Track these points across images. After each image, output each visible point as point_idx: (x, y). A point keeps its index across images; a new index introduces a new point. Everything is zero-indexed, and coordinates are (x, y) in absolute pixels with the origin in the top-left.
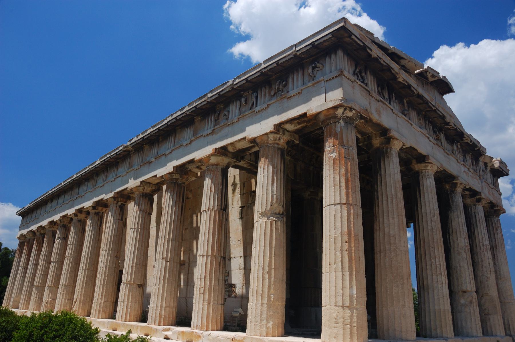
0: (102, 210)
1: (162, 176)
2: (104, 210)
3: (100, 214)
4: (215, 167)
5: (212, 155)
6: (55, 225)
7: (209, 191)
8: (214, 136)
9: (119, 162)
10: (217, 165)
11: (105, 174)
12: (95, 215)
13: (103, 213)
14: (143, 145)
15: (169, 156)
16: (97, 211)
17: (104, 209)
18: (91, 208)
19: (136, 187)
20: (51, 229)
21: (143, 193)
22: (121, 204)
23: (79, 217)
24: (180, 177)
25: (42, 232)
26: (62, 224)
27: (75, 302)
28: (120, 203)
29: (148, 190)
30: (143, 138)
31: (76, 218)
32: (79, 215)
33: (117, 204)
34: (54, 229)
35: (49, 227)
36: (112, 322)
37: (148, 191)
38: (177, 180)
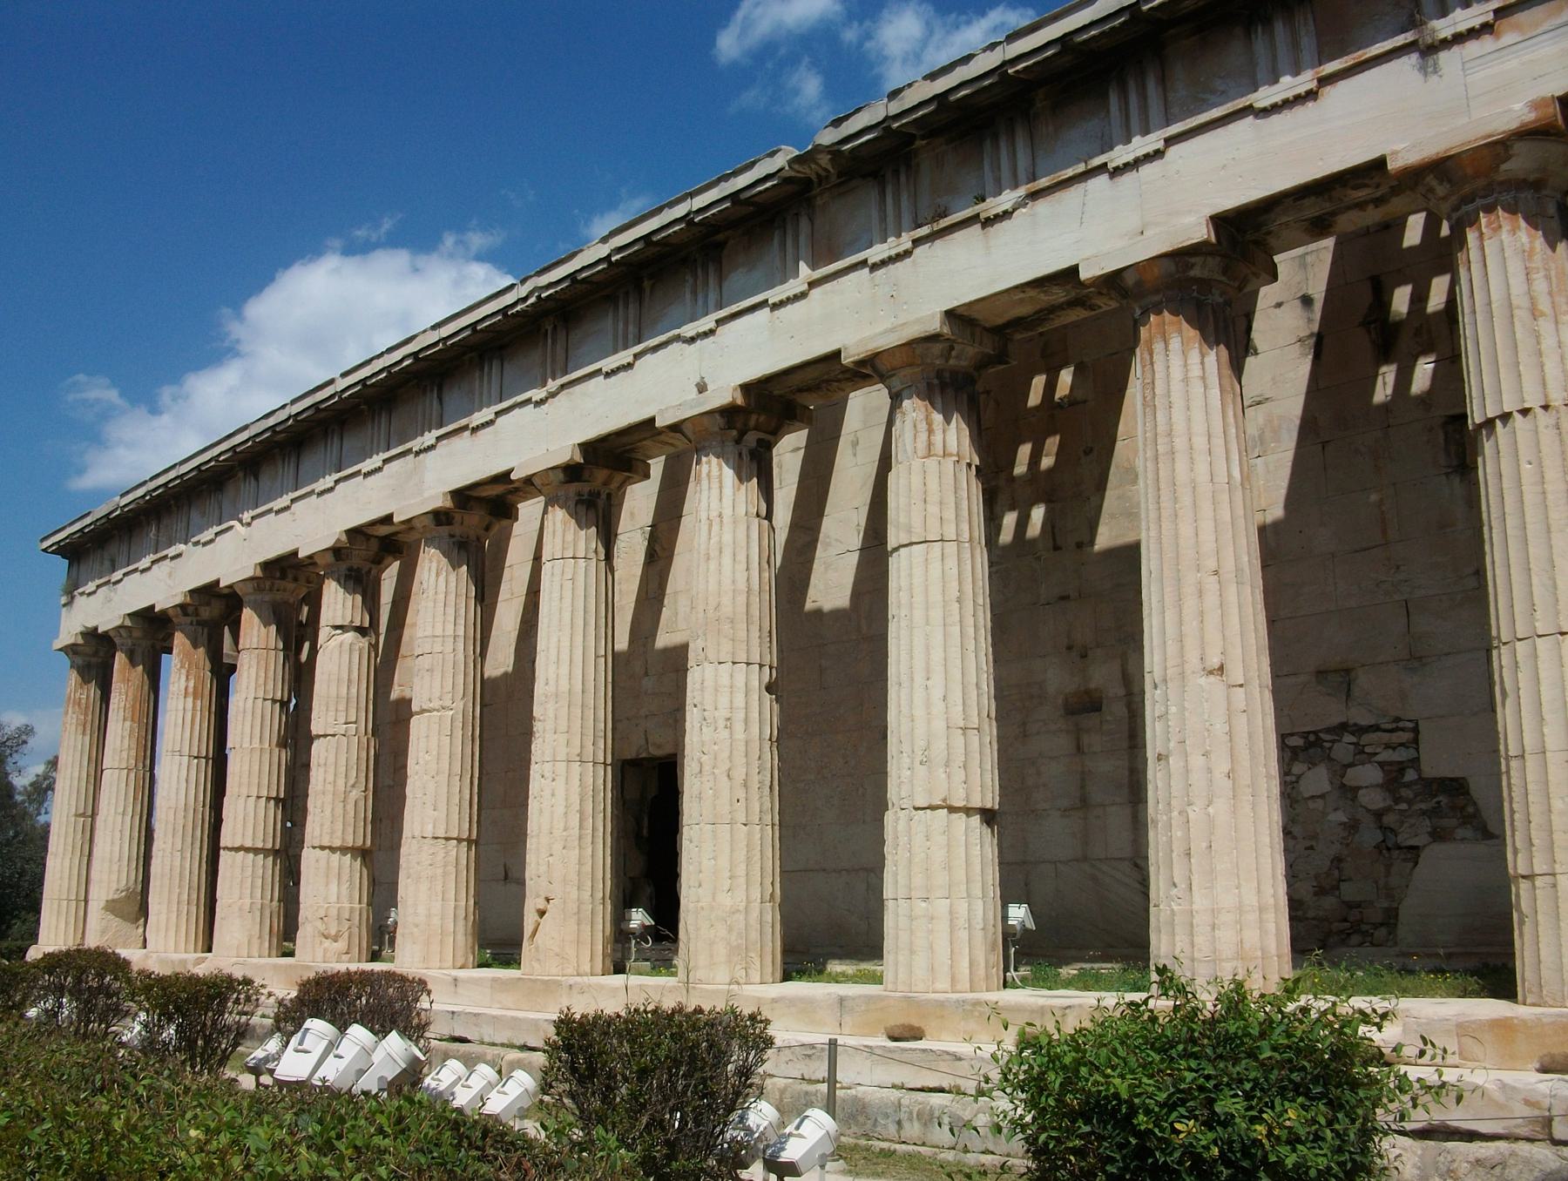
0: (605, 484)
1: (1119, 273)
2: (614, 485)
3: (601, 503)
4: (1527, 195)
5: (1527, 134)
6: (283, 577)
7: (1521, 315)
8: (1508, 38)
9: (721, 246)
10: (1537, 185)
11: (632, 310)
12: (582, 509)
13: (609, 496)
14: (911, 138)
15: (1147, 170)
16: (585, 488)
17: (619, 477)
18: (561, 476)
19: (910, 344)
20: (267, 598)
21: (939, 374)
22: (759, 441)
23: (457, 529)
24: (1225, 272)
25: (206, 613)
26: (343, 566)
27: (542, 913)
28: (751, 438)
29: (967, 353)
30: (941, 98)
31: (445, 530)
32: (458, 517)
33: (738, 442)
34: (278, 596)
35: (259, 589)
36: (869, 999)
37: (964, 363)
38: (1205, 284)
